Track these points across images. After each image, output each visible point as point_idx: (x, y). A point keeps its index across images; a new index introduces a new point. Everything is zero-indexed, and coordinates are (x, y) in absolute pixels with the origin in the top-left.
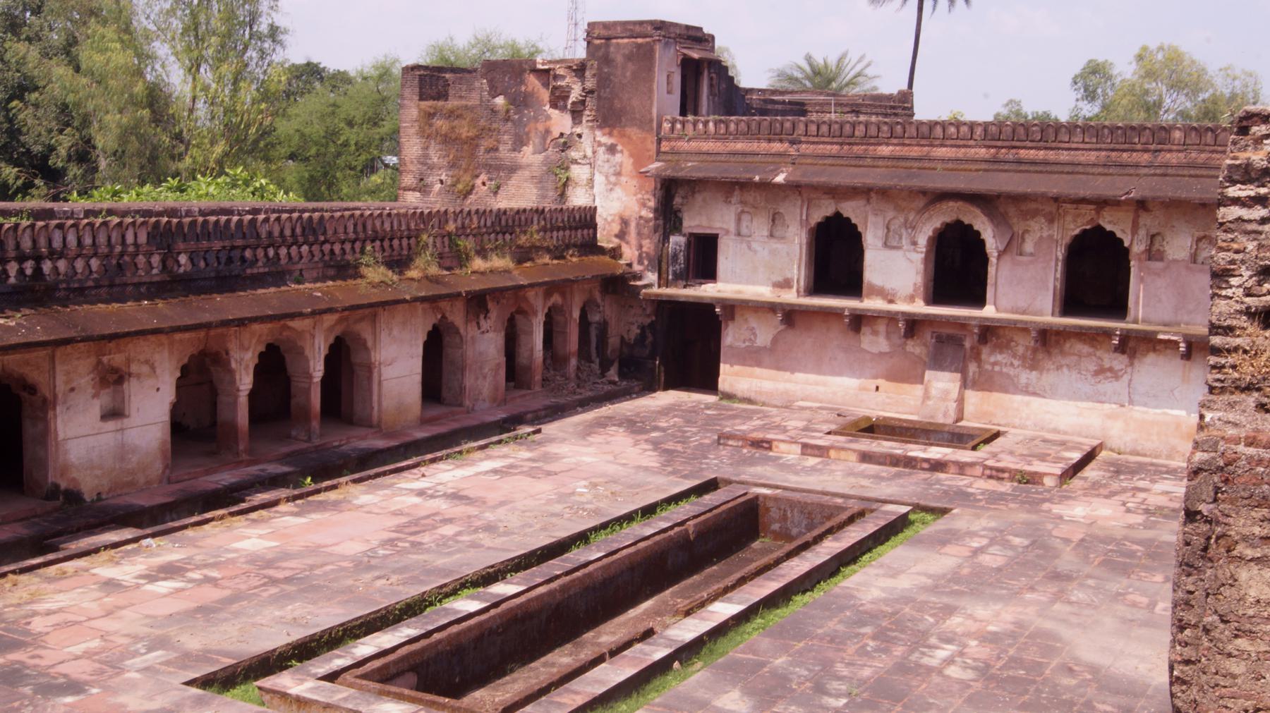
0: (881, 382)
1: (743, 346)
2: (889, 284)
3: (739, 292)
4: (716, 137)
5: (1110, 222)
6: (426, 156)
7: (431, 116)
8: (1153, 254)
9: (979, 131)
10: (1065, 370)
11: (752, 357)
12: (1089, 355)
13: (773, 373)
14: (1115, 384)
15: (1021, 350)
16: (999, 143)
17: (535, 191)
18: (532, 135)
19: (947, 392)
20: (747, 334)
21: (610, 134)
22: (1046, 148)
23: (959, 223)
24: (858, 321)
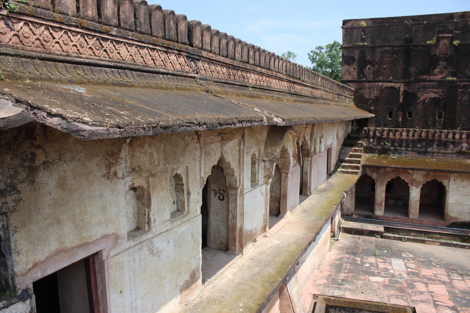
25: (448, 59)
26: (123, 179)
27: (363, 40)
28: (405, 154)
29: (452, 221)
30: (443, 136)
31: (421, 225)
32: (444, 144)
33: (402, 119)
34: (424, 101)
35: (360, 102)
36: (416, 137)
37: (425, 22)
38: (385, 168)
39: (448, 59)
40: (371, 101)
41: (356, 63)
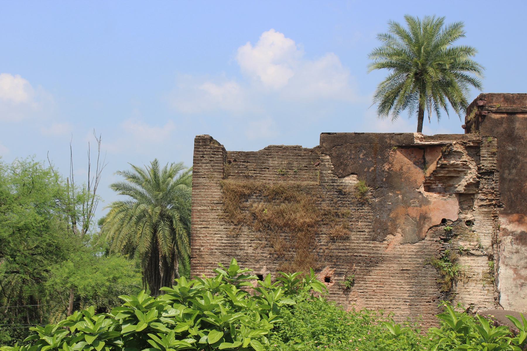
6: (237, 246)
7: (245, 197)
17: (407, 287)
18: (401, 221)
21: (520, 221)
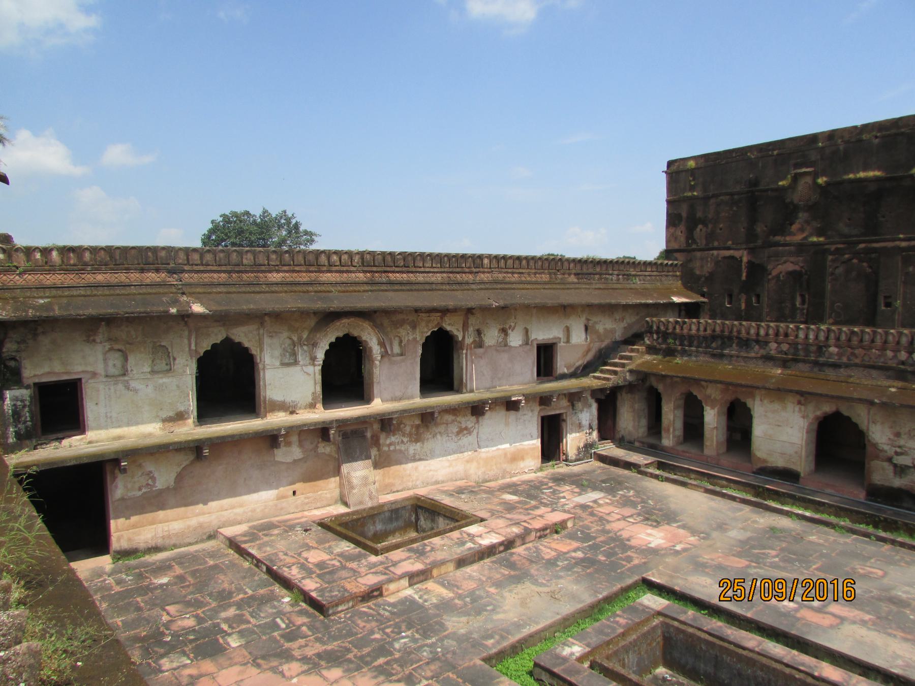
0: (298, 486)
1: (140, 493)
2: (290, 397)
3: (120, 438)
4: (65, 268)
5: (449, 324)
8: (480, 344)
9: (357, 259)
10: (438, 436)
11: (154, 501)
12: (453, 421)
13: (181, 510)
14: (470, 438)
15: (408, 429)
16: (375, 269)
19: (365, 478)
20: (143, 481)
22: (408, 272)
23: (347, 337)
24: (271, 439)
25: (812, 208)
26: (101, 343)
27: (692, 188)
28: (696, 356)
29: (759, 465)
30: (743, 331)
31: (718, 466)
32: (745, 343)
33: (746, 305)
34: (778, 276)
35: (690, 282)
36: (709, 332)
37: (775, 153)
38: (672, 377)
39: (812, 208)
40: (703, 279)
41: (683, 223)
